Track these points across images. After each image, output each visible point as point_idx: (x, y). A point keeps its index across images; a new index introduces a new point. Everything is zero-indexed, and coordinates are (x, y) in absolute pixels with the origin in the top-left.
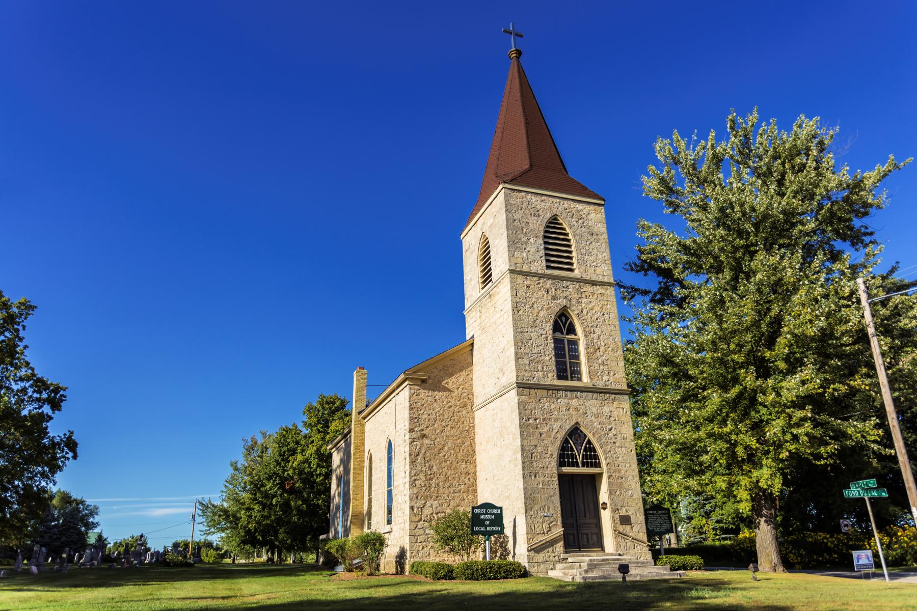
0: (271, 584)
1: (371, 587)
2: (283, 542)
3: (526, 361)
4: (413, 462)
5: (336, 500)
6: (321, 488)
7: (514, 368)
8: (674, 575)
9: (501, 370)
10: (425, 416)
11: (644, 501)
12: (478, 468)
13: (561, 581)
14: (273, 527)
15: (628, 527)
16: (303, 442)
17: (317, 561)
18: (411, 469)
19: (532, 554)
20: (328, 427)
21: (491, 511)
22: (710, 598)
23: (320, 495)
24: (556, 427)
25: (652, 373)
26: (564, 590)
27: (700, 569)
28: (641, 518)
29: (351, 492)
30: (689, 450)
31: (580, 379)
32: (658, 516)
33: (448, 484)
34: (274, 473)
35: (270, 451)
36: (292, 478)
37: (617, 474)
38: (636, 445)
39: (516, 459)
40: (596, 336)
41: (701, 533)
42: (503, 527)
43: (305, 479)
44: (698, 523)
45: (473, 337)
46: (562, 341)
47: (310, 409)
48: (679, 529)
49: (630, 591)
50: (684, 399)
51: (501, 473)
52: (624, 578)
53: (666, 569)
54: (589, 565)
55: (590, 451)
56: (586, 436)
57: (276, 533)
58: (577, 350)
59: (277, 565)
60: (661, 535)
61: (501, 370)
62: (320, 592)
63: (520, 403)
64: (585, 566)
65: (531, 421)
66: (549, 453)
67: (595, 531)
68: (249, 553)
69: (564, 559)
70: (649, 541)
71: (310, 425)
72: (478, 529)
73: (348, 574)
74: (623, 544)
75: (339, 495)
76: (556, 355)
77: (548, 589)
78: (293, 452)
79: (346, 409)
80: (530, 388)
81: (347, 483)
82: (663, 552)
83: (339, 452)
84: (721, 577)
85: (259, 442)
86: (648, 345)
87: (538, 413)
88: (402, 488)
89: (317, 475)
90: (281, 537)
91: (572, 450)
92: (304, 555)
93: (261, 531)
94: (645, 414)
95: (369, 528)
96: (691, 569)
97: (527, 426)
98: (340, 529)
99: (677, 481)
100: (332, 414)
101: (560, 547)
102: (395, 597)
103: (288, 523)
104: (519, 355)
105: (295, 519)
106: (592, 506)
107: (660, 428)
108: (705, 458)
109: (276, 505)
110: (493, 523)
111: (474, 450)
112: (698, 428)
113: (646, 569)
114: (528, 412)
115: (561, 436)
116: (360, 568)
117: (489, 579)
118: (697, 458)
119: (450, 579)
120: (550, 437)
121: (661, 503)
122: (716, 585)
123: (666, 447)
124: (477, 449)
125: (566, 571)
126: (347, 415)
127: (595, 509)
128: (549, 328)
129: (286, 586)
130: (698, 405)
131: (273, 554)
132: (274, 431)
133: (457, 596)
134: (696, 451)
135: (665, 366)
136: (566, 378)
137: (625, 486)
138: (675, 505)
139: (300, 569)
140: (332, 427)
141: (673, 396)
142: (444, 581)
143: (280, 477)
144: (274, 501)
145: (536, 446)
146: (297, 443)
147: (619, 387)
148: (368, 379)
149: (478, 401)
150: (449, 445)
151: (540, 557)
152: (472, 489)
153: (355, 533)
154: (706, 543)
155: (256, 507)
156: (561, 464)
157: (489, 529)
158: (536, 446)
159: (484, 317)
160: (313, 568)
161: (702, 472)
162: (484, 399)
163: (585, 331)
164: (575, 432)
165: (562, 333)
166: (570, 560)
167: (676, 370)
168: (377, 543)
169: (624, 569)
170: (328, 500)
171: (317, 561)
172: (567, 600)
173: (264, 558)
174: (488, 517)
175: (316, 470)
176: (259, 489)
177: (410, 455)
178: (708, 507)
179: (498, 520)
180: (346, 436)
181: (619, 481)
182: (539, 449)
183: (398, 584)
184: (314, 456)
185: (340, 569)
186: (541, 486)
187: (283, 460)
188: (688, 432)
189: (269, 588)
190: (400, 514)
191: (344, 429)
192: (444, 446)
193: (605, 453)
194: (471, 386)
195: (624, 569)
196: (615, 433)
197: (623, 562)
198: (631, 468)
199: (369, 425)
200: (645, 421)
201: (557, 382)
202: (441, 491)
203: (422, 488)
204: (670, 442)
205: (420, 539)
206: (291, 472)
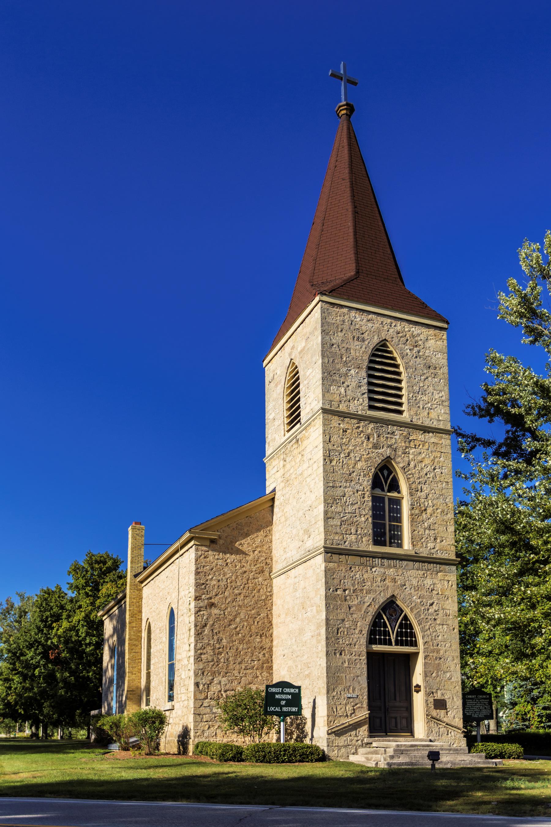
0: (36, 762)
1: (150, 767)
2: (48, 716)
3: (337, 522)
4: (199, 634)
5: (110, 673)
6: (92, 659)
7: (322, 529)
8: (489, 763)
9: (307, 532)
10: (214, 582)
11: (463, 682)
12: (275, 643)
13: (362, 766)
14: (36, 699)
15: (443, 712)
16: (68, 607)
17: (88, 737)
18: (196, 641)
19: (333, 737)
20: (99, 591)
21: (288, 690)
22: (526, 789)
23: (90, 667)
24: (368, 599)
25: (486, 541)
26: (366, 776)
27: (518, 758)
28: (459, 702)
29: (127, 665)
30: (521, 631)
31: (400, 546)
32: (478, 701)
33: (239, 660)
34: (36, 641)
35: (29, 615)
36: (57, 647)
37: (435, 654)
38: (461, 622)
39: (319, 634)
40: (423, 494)
41: (524, 720)
42: (300, 708)
43: (72, 648)
44: (522, 709)
45: (274, 490)
46: (382, 500)
47: (76, 569)
48: (501, 714)
49: (439, 779)
50: (522, 573)
51: (301, 647)
52: (433, 765)
53: (480, 757)
54: (395, 751)
55: (406, 629)
56: (402, 611)
57: (40, 707)
58: (399, 511)
59: (42, 741)
60: (479, 721)
61: (307, 532)
62: (92, 772)
63: (327, 571)
64: (390, 751)
65: (339, 592)
66: (359, 629)
67: (405, 714)
68: (10, 727)
69: (367, 744)
70: (465, 727)
71: (77, 587)
72: (272, 709)
73: (124, 753)
74: (435, 729)
75: (113, 667)
76: (374, 516)
77: (348, 775)
78: (57, 618)
79: (120, 570)
80: (340, 554)
81: (122, 655)
82: (479, 738)
83: (111, 620)
84: (540, 767)
85: (16, 606)
86: (485, 509)
87: (348, 583)
88: (185, 662)
89: (86, 645)
90: (45, 711)
91: (385, 626)
92: (74, 731)
93: (22, 704)
94: (473, 588)
95: (147, 704)
96: (509, 758)
97: (334, 597)
98: (114, 704)
99: (502, 665)
100: (103, 575)
101: (364, 731)
102: (176, 779)
103: (54, 696)
104: (329, 515)
105: (62, 692)
106: (403, 689)
107: (490, 605)
108: (539, 641)
109: (39, 676)
110: (289, 703)
111: (270, 622)
112: (533, 607)
113: (456, 753)
114: (336, 582)
115: (372, 611)
116: (137, 746)
117: (283, 762)
118: (529, 639)
119: (238, 761)
120: (360, 610)
121: (482, 686)
122: (535, 776)
123: (494, 626)
124: (274, 622)
125: (370, 756)
126: (120, 577)
127: (407, 691)
128: (367, 483)
129: (53, 764)
130: (537, 579)
131: (37, 729)
132: (34, 594)
133: (246, 779)
134: (529, 631)
135: (503, 533)
136: (383, 544)
137: (444, 667)
138: (499, 689)
139: (69, 746)
140: (103, 590)
141: (509, 568)
142: (232, 763)
143: (43, 645)
144: (37, 672)
145: (343, 620)
146: (62, 607)
147: (445, 556)
148: (146, 536)
149: (277, 567)
150: (242, 615)
151: (341, 741)
152: (267, 665)
153: (131, 710)
154: (529, 730)
155: (16, 678)
156: (371, 641)
157: (285, 709)
158: (343, 620)
159: (288, 466)
160: (84, 745)
161: (534, 655)
162: (284, 564)
163: (410, 488)
164: (390, 607)
165: (383, 490)
166: (374, 744)
167: (515, 538)
168: (157, 721)
169: (434, 756)
170: (100, 672)
171: (88, 737)
172: (368, 786)
173: (28, 732)
174: (284, 697)
175: (84, 639)
176: (18, 658)
177: (196, 626)
178: (535, 693)
179: (296, 700)
180: (119, 602)
181: (437, 662)
182: (347, 624)
183: (180, 765)
184: (82, 622)
185: (115, 747)
186: (346, 665)
187: (45, 626)
188: (523, 610)
189: (34, 766)
190: (183, 690)
191: (117, 593)
192: (236, 617)
193: (423, 630)
194: (270, 549)
195: (434, 756)
196: (437, 606)
197: (434, 749)
198: (451, 647)
199: (147, 591)
200: (472, 596)
201: (372, 548)
202: (231, 667)
203: (211, 658)
204: (499, 622)
205: (206, 718)
206: (55, 641)
